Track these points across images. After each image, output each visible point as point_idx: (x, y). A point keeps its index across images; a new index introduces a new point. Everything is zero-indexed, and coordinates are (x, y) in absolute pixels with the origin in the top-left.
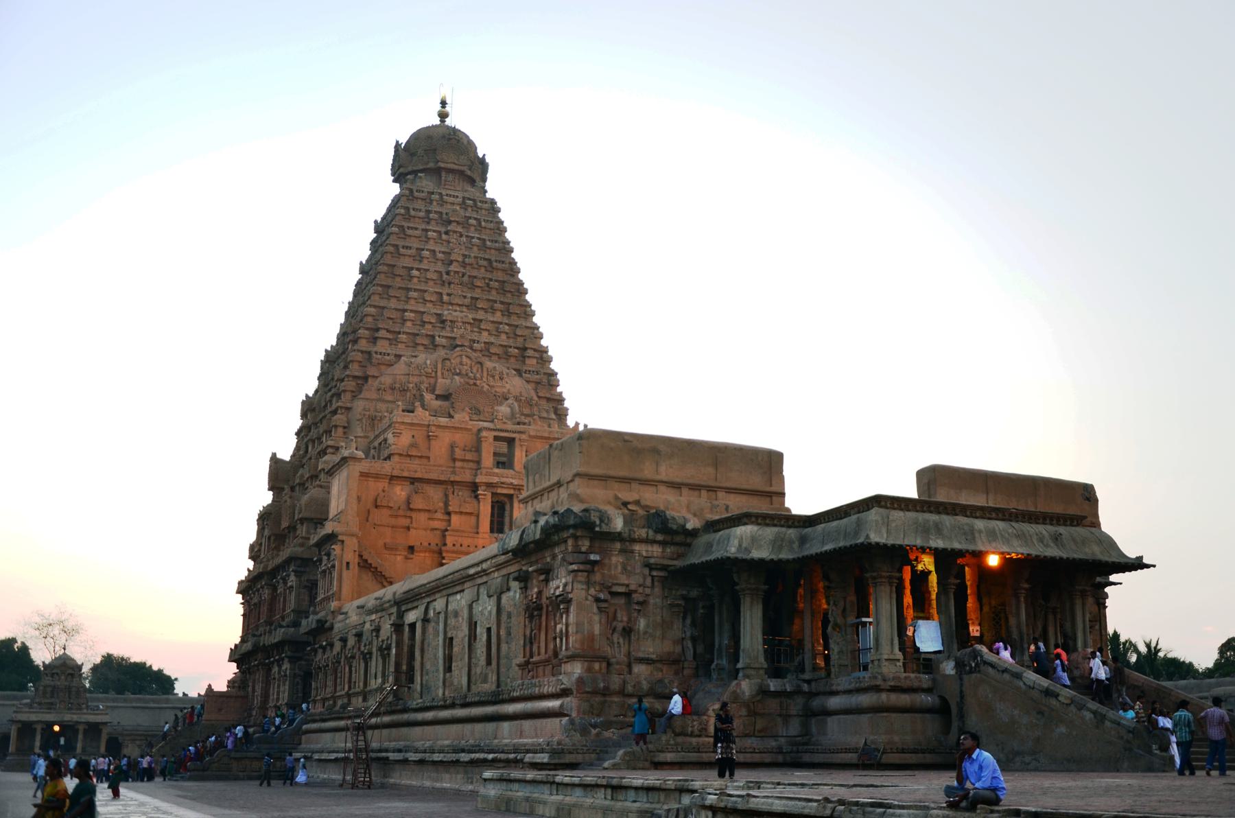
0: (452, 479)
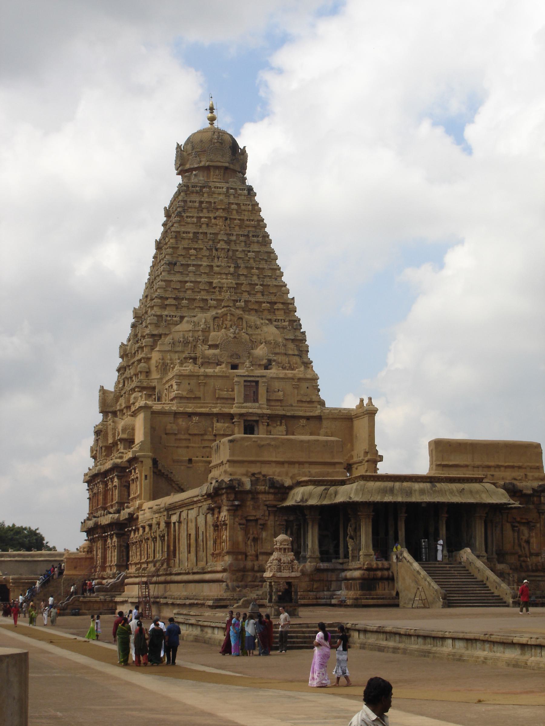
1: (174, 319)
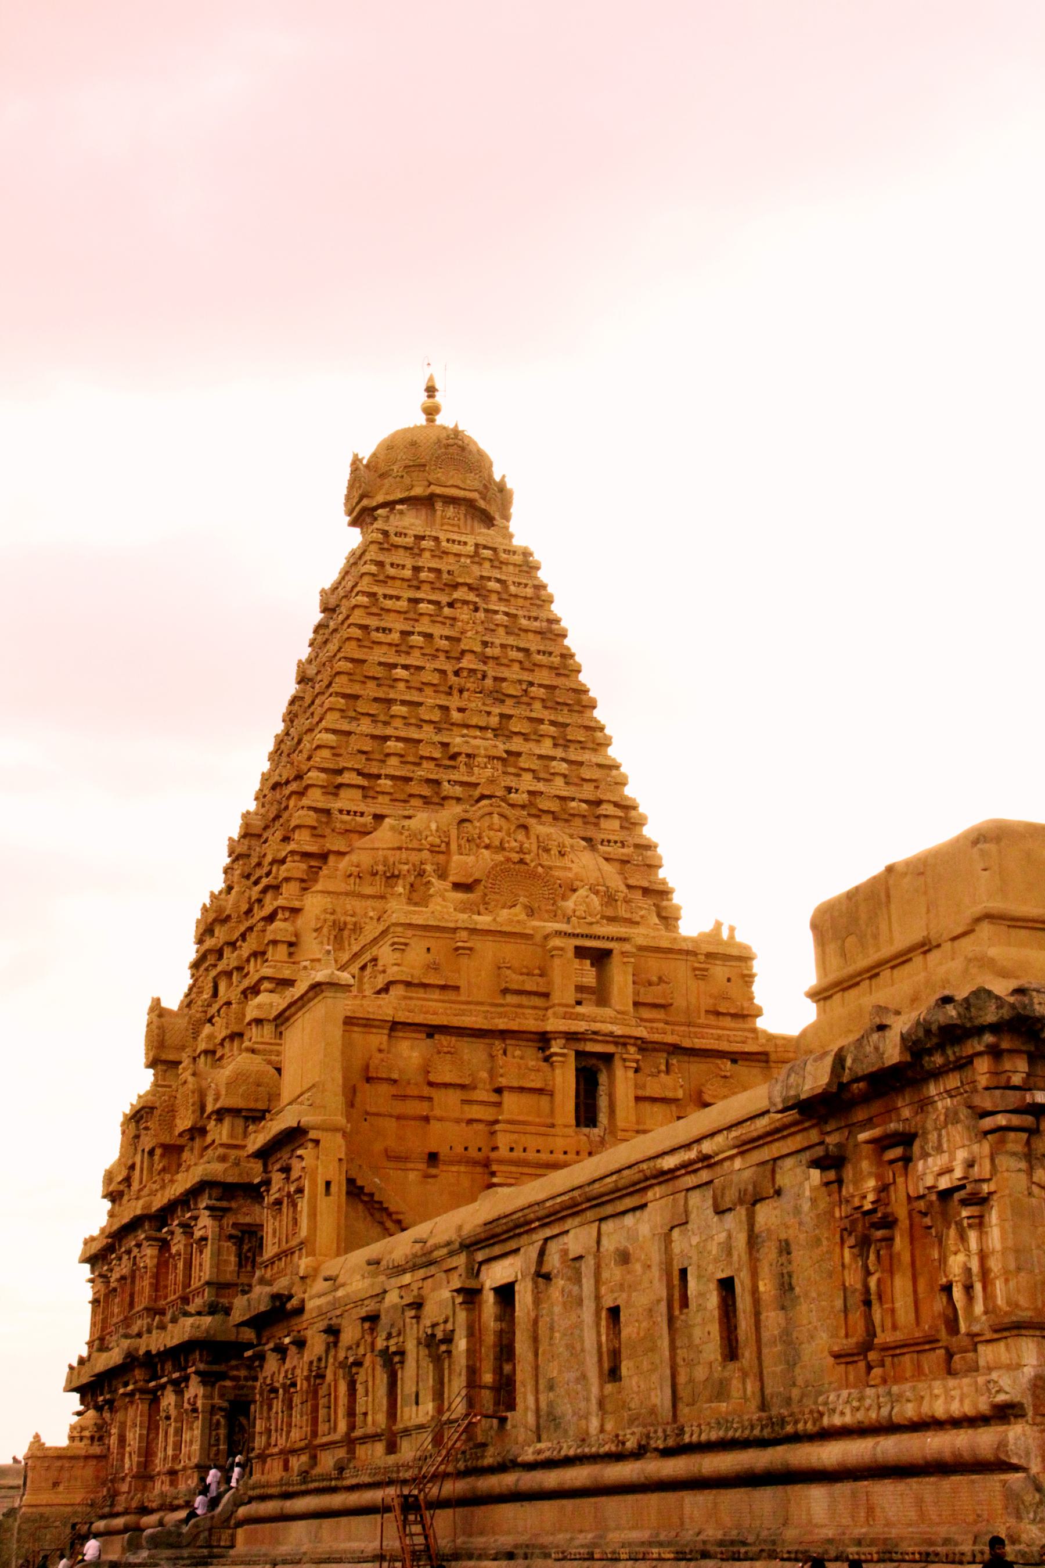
0: (502, 1027)
1: (358, 818)
